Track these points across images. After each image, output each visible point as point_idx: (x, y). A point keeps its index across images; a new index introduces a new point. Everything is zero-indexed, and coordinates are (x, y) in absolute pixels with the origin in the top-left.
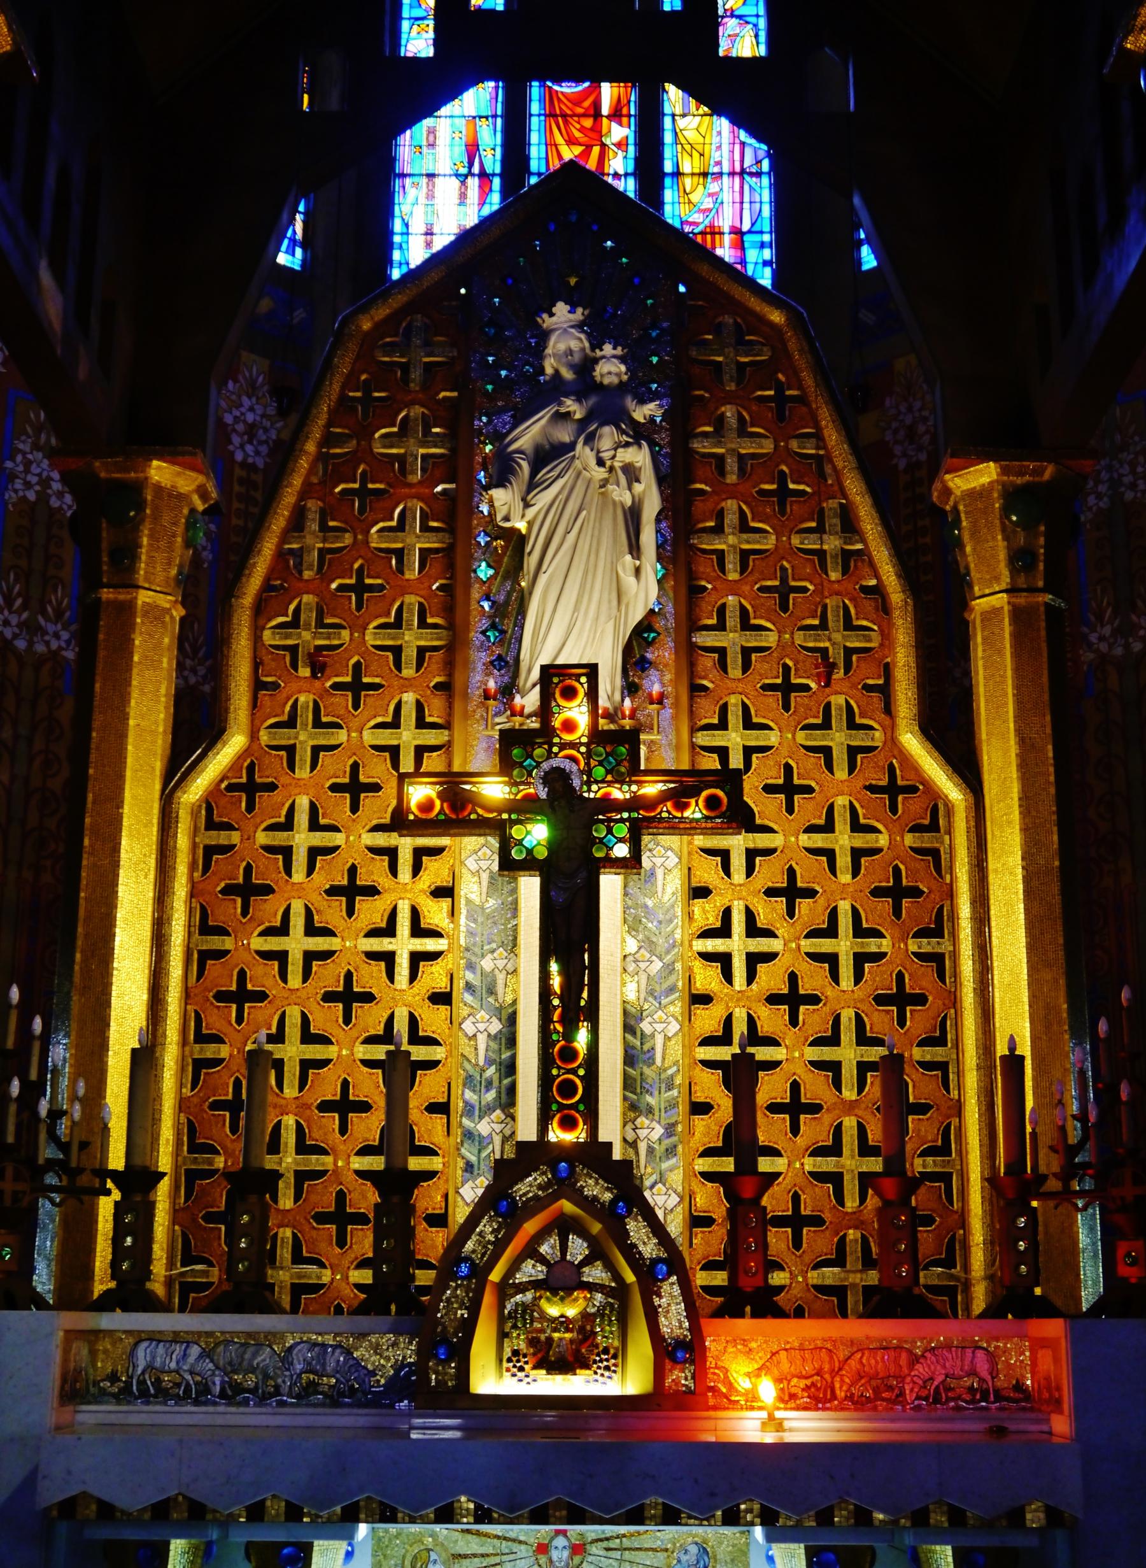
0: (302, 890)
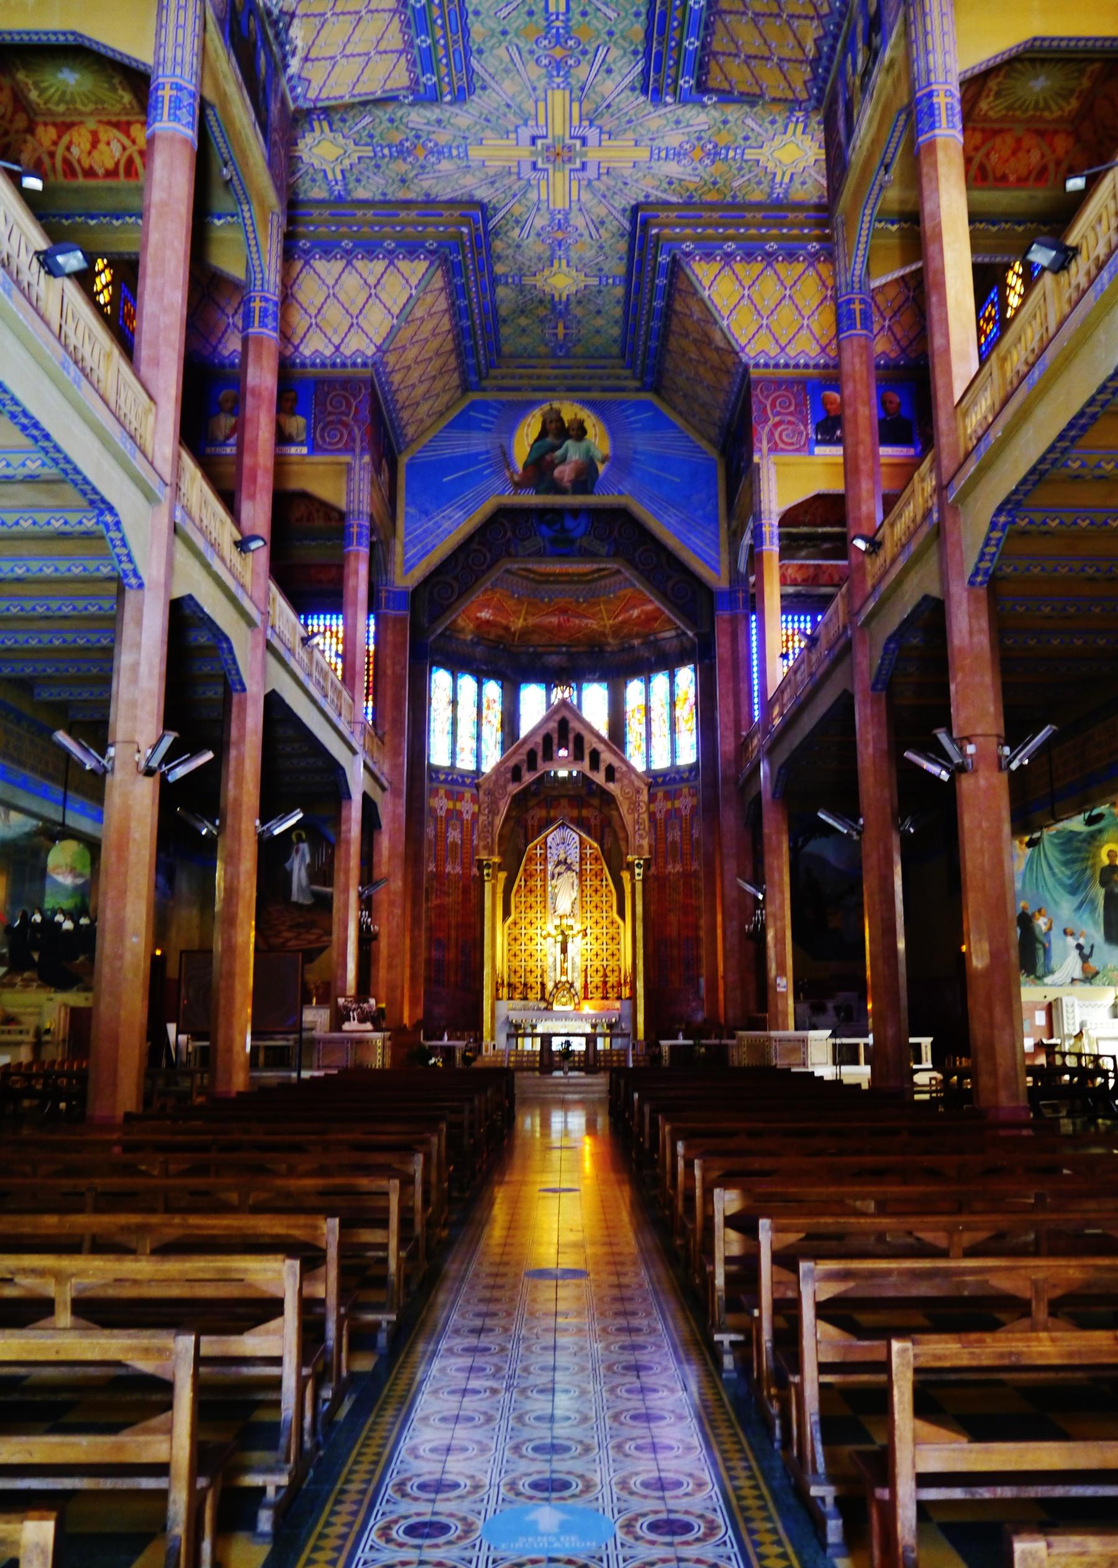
0: (523, 939)
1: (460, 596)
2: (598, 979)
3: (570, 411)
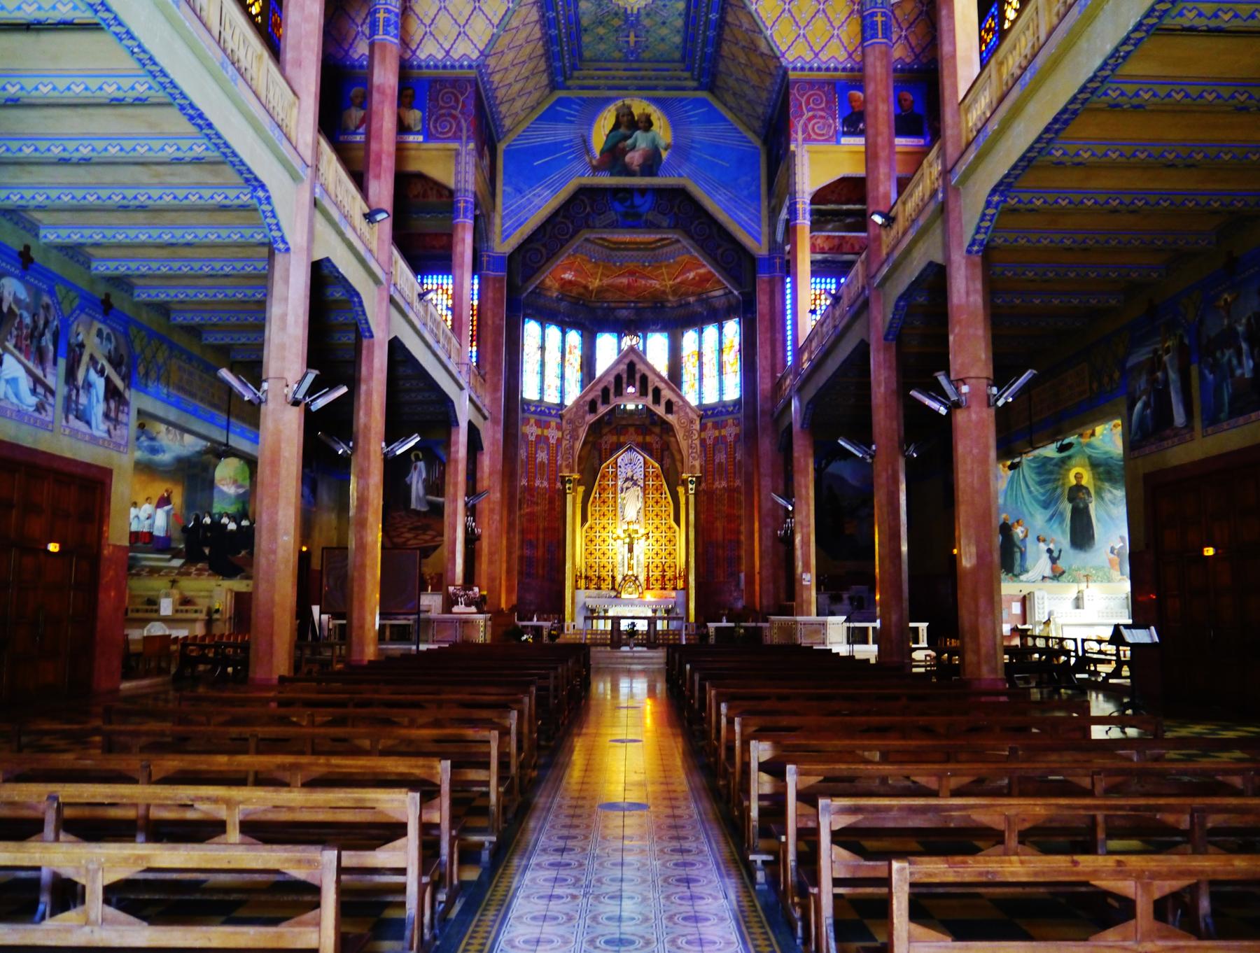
0: (598, 541)
1: (547, 260)
2: (657, 574)
3: (639, 107)
